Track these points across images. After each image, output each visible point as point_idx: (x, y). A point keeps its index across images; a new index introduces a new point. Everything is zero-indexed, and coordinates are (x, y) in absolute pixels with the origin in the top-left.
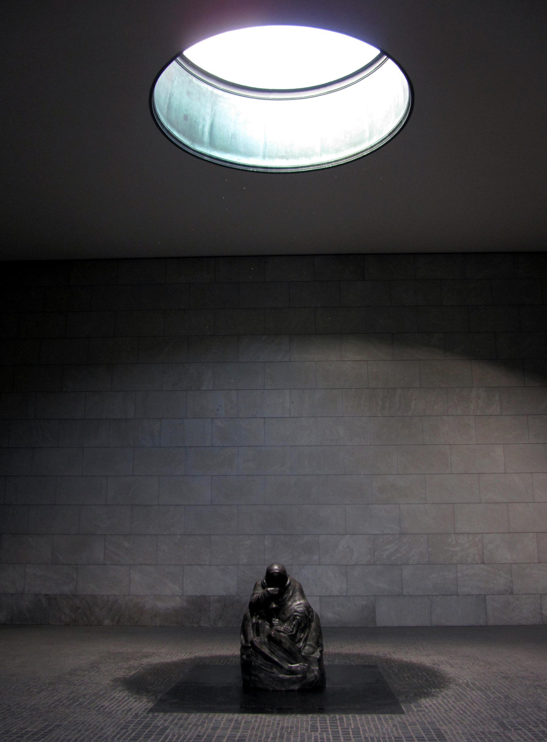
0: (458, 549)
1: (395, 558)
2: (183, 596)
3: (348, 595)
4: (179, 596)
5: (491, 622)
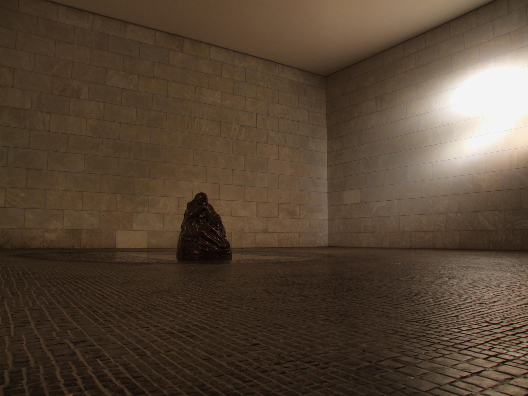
0: (220, 208)
2: (63, 229)
3: (164, 230)
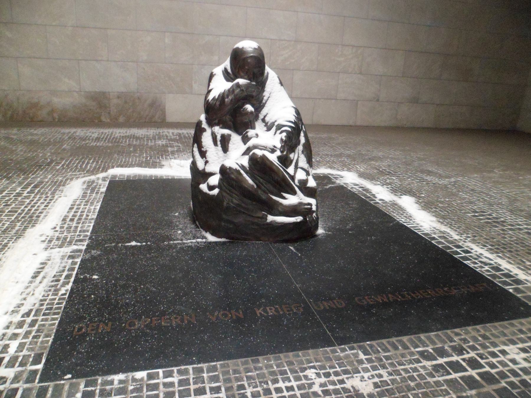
0: (342, 59)
1: (289, 63)
2: (81, 91)
4: (76, 92)
5: (358, 123)
